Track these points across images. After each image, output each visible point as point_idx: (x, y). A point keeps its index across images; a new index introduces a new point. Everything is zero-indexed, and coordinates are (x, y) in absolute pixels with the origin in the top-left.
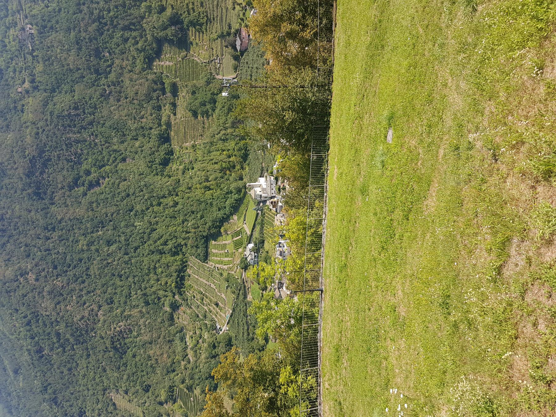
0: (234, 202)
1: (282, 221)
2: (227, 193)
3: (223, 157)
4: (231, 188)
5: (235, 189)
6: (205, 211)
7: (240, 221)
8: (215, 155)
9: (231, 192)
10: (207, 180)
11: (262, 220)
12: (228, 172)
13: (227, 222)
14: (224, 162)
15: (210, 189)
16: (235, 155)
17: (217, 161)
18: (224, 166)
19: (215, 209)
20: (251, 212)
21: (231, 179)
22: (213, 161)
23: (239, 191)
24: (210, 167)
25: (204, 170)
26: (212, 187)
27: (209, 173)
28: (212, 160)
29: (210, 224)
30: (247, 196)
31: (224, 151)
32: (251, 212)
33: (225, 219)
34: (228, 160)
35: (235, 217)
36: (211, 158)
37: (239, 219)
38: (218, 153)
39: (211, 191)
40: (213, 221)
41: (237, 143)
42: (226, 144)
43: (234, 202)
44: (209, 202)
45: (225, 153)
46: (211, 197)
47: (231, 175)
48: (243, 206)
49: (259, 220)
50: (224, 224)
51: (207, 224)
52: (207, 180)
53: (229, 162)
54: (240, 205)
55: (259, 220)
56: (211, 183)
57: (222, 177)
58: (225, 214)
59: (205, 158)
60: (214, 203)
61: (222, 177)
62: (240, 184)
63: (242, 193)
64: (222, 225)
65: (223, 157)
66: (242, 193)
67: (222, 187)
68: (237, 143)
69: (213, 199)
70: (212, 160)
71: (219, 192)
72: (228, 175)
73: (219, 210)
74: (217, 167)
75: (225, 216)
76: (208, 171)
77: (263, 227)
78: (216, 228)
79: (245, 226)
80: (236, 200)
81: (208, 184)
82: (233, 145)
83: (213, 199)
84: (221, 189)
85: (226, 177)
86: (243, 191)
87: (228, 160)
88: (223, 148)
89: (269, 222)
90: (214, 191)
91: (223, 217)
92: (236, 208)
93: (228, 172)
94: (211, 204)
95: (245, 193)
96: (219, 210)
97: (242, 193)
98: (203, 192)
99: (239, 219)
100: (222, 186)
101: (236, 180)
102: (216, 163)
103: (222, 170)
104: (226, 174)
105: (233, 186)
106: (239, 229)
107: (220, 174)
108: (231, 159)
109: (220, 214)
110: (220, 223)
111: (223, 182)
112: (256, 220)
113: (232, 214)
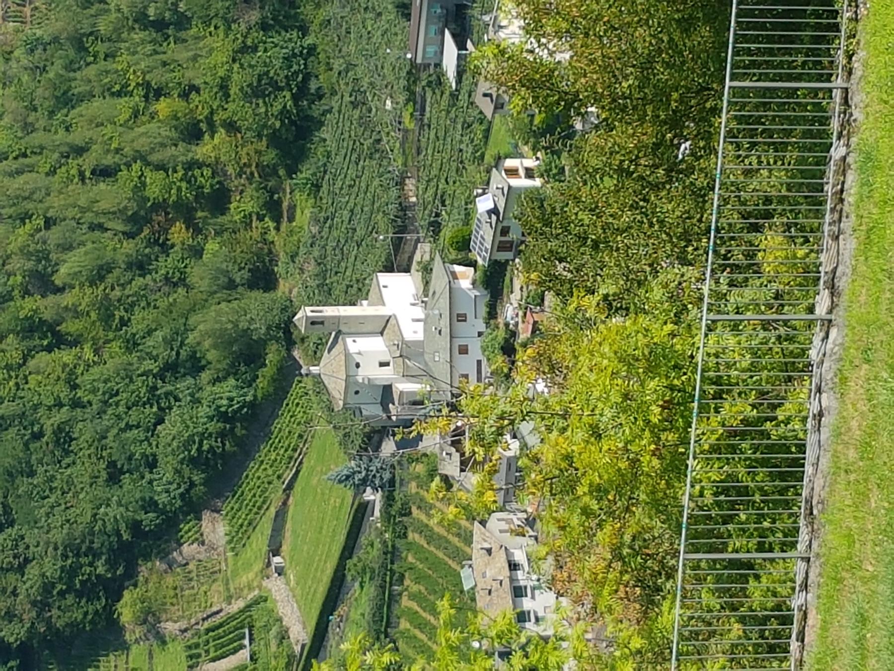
0: (214, 427)
1: (519, 556)
2: (171, 369)
3: (152, 133)
4: (191, 338)
5: (224, 341)
6: (23, 485)
7: (248, 554)
8: (102, 123)
9: (196, 365)
10: (42, 282)
11: (392, 554)
12: (178, 234)
13: (164, 555)
14: (161, 167)
15: (59, 341)
16: (231, 127)
17: (109, 160)
18: (154, 191)
19: (83, 468)
20: (318, 497)
21: (200, 275)
22: (88, 162)
23: (246, 354)
24: (68, 197)
25: (24, 217)
26: (70, 327)
27: (54, 235)
28: (80, 151)
29: (51, 567)
30: (295, 390)
31: (159, 93)
32: (318, 497)
33: (151, 538)
34: (180, 153)
35: (215, 528)
36: (77, 137)
37: (239, 538)
38: (123, 107)
39: (66, 356)
40: (71, 549)
41: (245, 49)
42: (174, 51)
43: (214, 427)
44: (50, 422)
45: (163, 107)
46: (64, 394)
47: (197, 252)
48: (267, 454)
49: (370, 552)
50: (144, 570)
51: (32, 571)
52: (42, 282)
53: (191, 165)
54: (246, 451)
55: (370, 552)
56: (67, 299)
57: (141, 266)
58: (150, 505)
59: (38, 138)
60: (84, 432)
61: (141, 266)
62: (254, 310)
63: (267, 367)
64: (131, 575)
65: (152, 133)
66: (267, 373)
67: (137, 325)
68: (245, 49)
69: (76, 404)
70: (80, 151)
71: (115, 357)
72: (176, 253)
73: (114, 476)
74: (111, 196)
75: (149, 519)
76: (49, 223)
77: (393, 599)
78: (87, 592)
79: (276, 587)
80: (223, 416)
81: (45, 306)
82: (221, 58)
83: (76, 404)
84: (132, 345)
85: (165, 265)
86: (273, 355)
87: (180, 153)
88: (156, 78)
89: (436, 564)
90: (88, 354)
91: (135, 526)
92: (220, 469)
93: (178, 234)
94: (64, 439)
95: (289, 371)
96: (114, 476)
97: (267, 373)
98: (15, 357)
99: (239, 538)
100: (140, 320)
101: (231, 285)
102: (105, 173)
103: (143, 218)
104: (166, 248)
105: (208, 325)
106: (238, 605)
107: (129, 247)
108: (204, 150)
109: (118, 509)
110: (112, 564)
111: (143, 299)
112: (348, 550)
113: (193, 507)
